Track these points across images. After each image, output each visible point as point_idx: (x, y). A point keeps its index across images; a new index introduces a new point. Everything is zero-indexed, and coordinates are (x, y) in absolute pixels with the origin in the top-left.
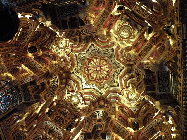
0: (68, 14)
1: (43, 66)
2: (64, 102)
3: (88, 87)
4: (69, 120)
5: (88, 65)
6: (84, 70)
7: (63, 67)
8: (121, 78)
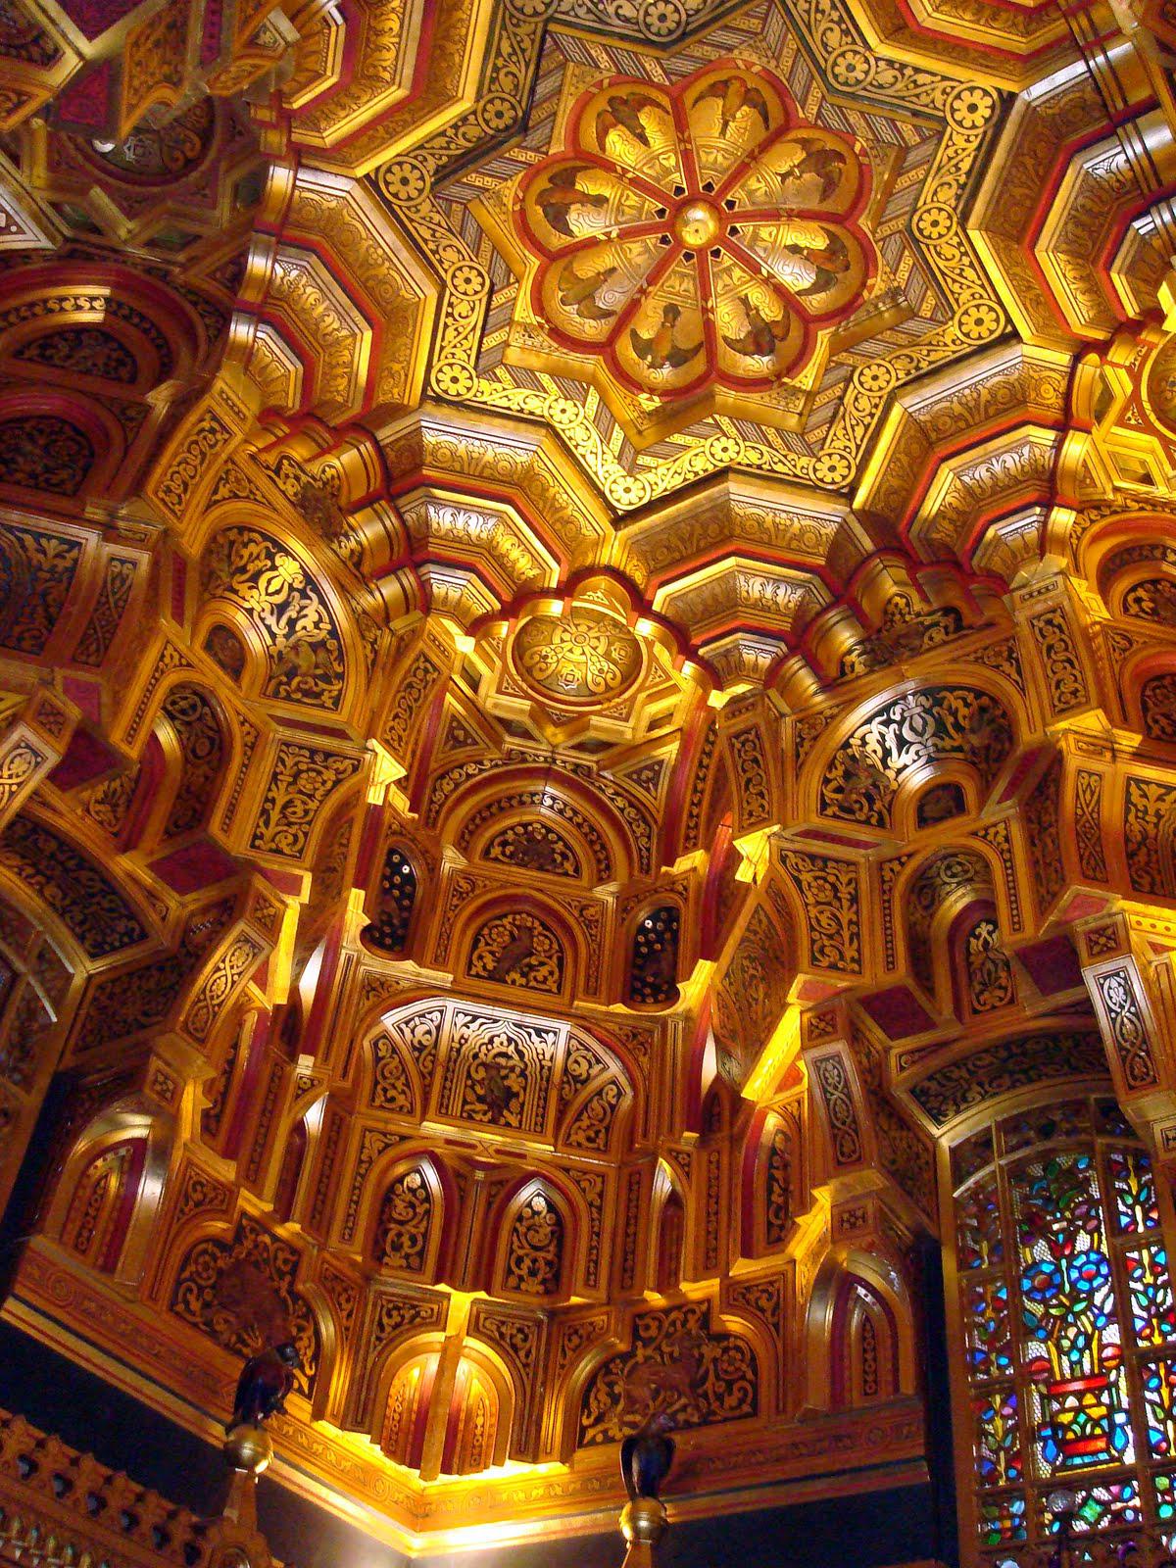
1: (76, 518)
2: (472, 725)
3: (664, 477)
4: (606, 893)
5: (557, 241)
6: (539, 305)
7: (292, 401)
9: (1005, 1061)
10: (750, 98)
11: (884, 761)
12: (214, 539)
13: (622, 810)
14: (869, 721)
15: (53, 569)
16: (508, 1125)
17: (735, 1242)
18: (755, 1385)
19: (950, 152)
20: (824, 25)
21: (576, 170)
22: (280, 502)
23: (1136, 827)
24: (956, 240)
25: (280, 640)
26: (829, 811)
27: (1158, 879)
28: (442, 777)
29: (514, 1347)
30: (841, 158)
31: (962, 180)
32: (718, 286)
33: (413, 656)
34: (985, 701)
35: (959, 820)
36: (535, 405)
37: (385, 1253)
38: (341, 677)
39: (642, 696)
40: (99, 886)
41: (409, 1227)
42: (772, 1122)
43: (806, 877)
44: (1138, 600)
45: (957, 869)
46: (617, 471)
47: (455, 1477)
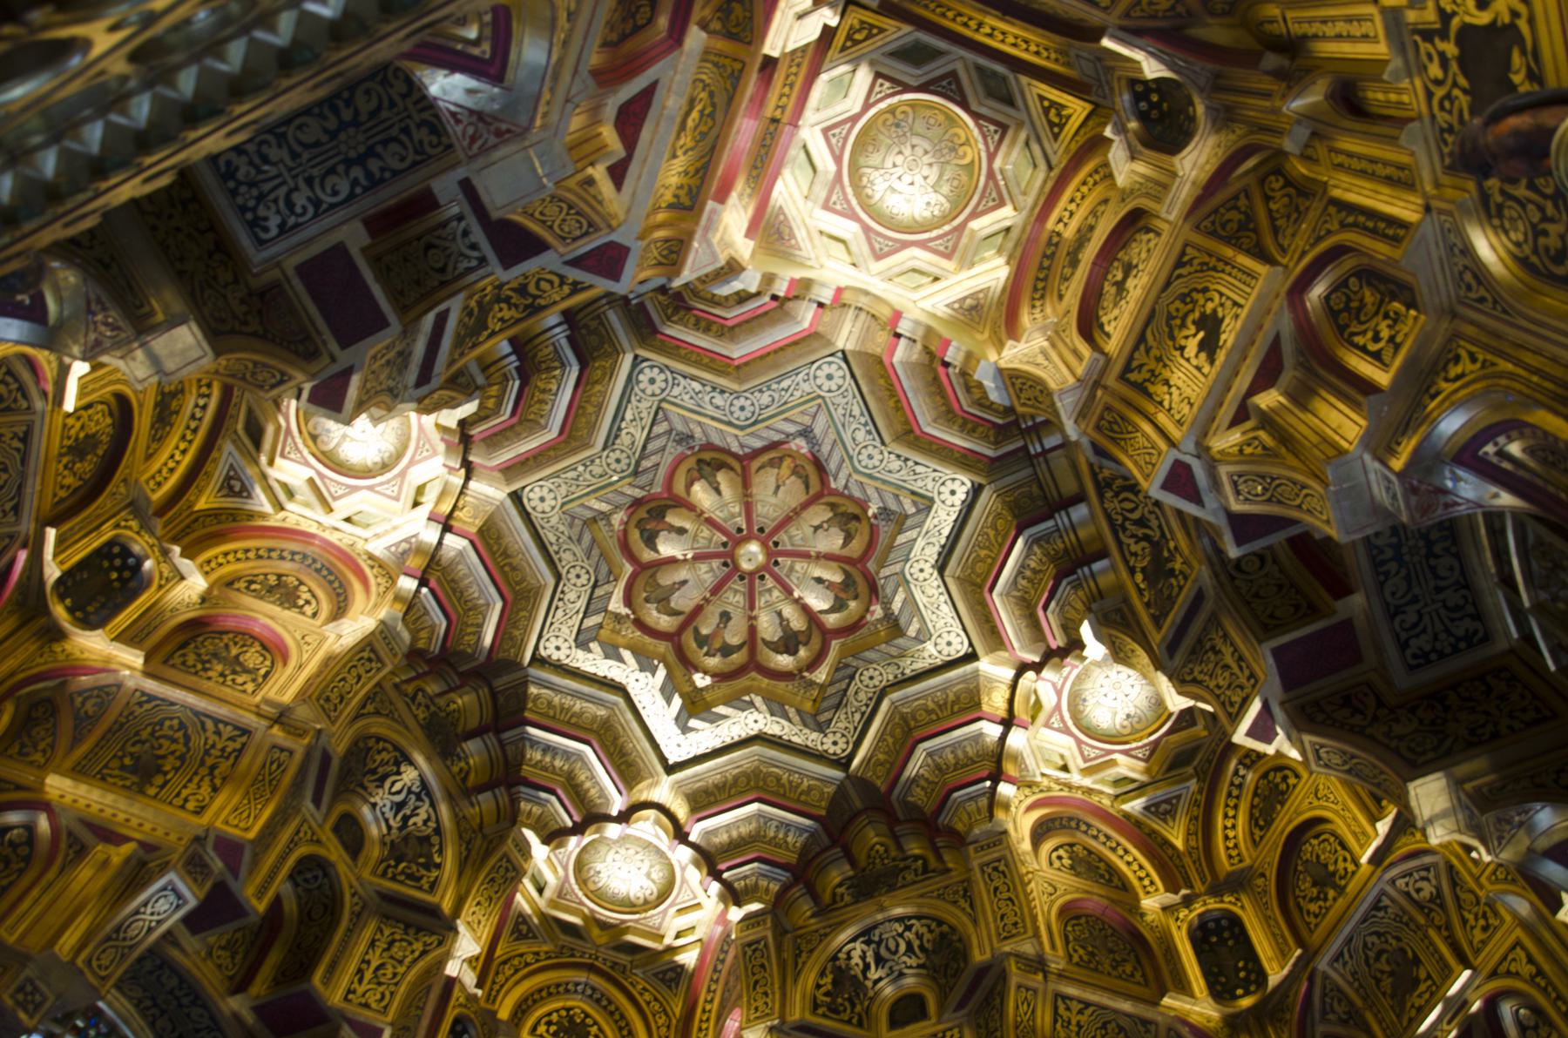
0: (344, 189)
3: (706, 737)
5: (647, 555)
6: (628, 600)
7: (435, 647)
10: (795, 471)
13: (648, 1003)
14: (854, 940)
15: (223, 750)
19: (936, 521)
22: (411, 723)
24: (935, 584)
25: (394, 831)
26: (820, 1011)
28: (505, 962)
30: (856, 518)
32: (761, 601)
34: (945, 928)
38: (438, 866)
44: (1060, 858)
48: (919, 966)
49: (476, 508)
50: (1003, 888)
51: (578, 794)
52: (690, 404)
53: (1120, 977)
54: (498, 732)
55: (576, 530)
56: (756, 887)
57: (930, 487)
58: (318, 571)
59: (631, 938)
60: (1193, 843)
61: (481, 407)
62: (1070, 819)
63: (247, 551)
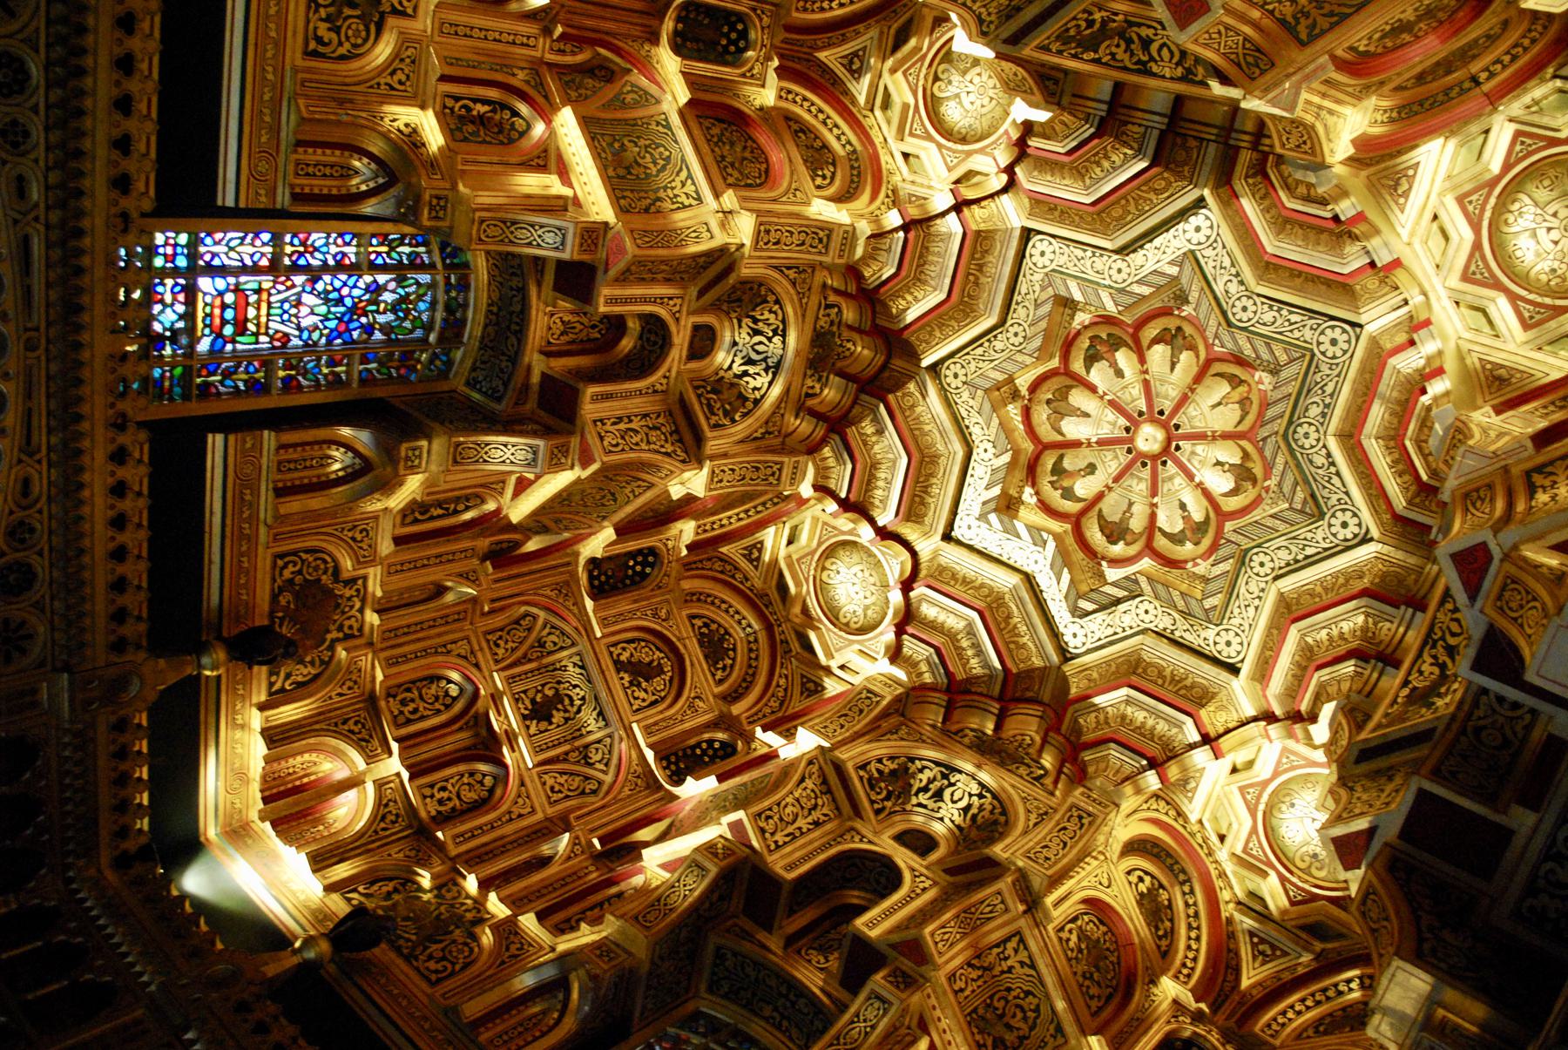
1: (717, 195)
3: (989, 536)
5: (1077, 366)
6: (1034, 387)
8: (1290, 611)
9: (780, 995)
10: (1244, 402)
11: (920, 790)
12: (761, 285)
14: (937, 764)
16: (528, 727)
17: (541, 905)
18: (453, 973)
19: (1309, 535)
20: (1316, 399)
21: (1127, 345)
23: (991, 958)
24: (1263, 585)
26: (862, 773)
27: (967, 993)
29: (383, 818)
30: (1254, 481)
31: (1300, 557)
33: (777, 459)
34: (1002, 819)
35: (915, 857)
36: (976, 432)
37: (394, 696)
38: (733, 421)
39: (857, 647)
40: (512, 353)
41: (422, 705)
42: (638, 880)
43: (809, 783)
44: (1141, 879)
45: (883, 880)
46: (977, 510)
47: (273, 834)
48: (958, 827)
49: (990, 218)
50: (1069, 833)
51: (869, 482)
52: (1208, 270)
53: (1081, 986)
54: (861, 390)
55: (1044, 296)
56: (915, 665)
57: (1330, 503)
58: (852, 167)
59: (813, 636)
60: (1254, 992)
61: (1051, 121)
62: (1183, 871)
63: (821, 111)
